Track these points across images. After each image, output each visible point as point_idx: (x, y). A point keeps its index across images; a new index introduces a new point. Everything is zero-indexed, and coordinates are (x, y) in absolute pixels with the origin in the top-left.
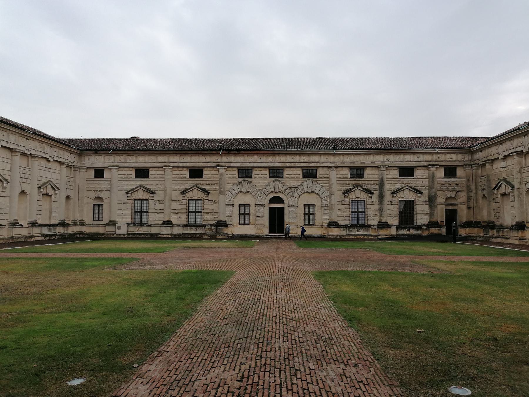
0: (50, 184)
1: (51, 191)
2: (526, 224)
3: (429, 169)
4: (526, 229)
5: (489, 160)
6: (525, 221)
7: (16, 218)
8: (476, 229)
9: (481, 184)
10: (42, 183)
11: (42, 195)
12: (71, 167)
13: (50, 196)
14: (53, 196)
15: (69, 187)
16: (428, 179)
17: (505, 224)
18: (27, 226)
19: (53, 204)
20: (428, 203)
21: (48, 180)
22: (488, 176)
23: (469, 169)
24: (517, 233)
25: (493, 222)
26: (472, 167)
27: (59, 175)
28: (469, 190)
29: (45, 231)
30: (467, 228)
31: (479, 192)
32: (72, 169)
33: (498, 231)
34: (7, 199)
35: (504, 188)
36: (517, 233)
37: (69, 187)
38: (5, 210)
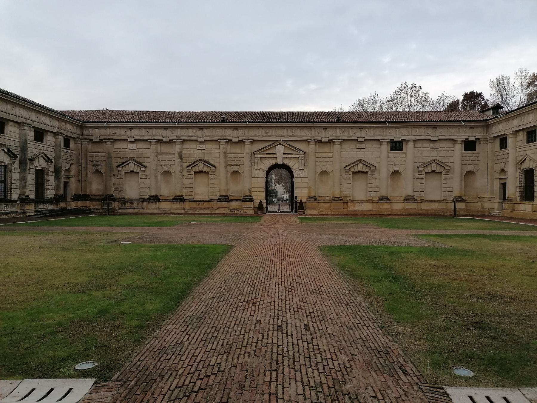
2: (159, 197)
3: (56, 137)
4: (161, 200)
5: (113, 139)
6: (159, 195)
8: (88, 202)
9: (65, 157)
16: (54, 148)
17: (126, 197)
20: (54, 174)
22: (109, 154)
23: (80, 142)
24: (156, 204)
25: (113, 196)
26: (82, 142)
28: (79, 163)
30: (79, 201)
31: (90, 167)
33: (131, 204)
35: (132, 166)
36: (156, 204)
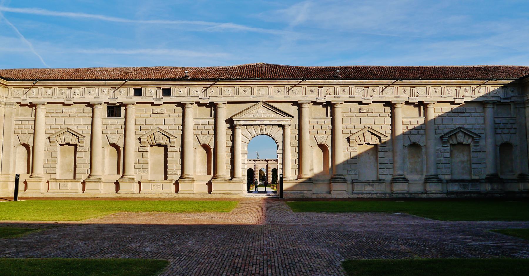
0: (461, 131)
1: (467, 140)
7: (400, 172)
10: (446, 131)
11: (449, 145)
12: (510, 105)
13: (469, 145)
14: (472, 144)
15: (506, 131)
18: (422, 182)
19: (473, 155)
21: (458, 126)
27: (483, 118)
29: (455, 188)
32: (512, 104)
34: (390, 154)
37: (506, 131)
38: (386, 165)
